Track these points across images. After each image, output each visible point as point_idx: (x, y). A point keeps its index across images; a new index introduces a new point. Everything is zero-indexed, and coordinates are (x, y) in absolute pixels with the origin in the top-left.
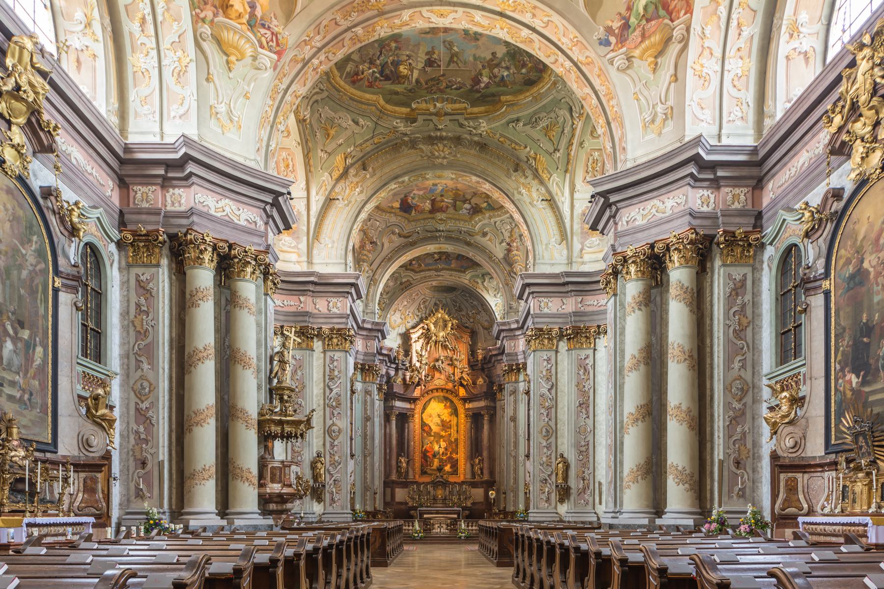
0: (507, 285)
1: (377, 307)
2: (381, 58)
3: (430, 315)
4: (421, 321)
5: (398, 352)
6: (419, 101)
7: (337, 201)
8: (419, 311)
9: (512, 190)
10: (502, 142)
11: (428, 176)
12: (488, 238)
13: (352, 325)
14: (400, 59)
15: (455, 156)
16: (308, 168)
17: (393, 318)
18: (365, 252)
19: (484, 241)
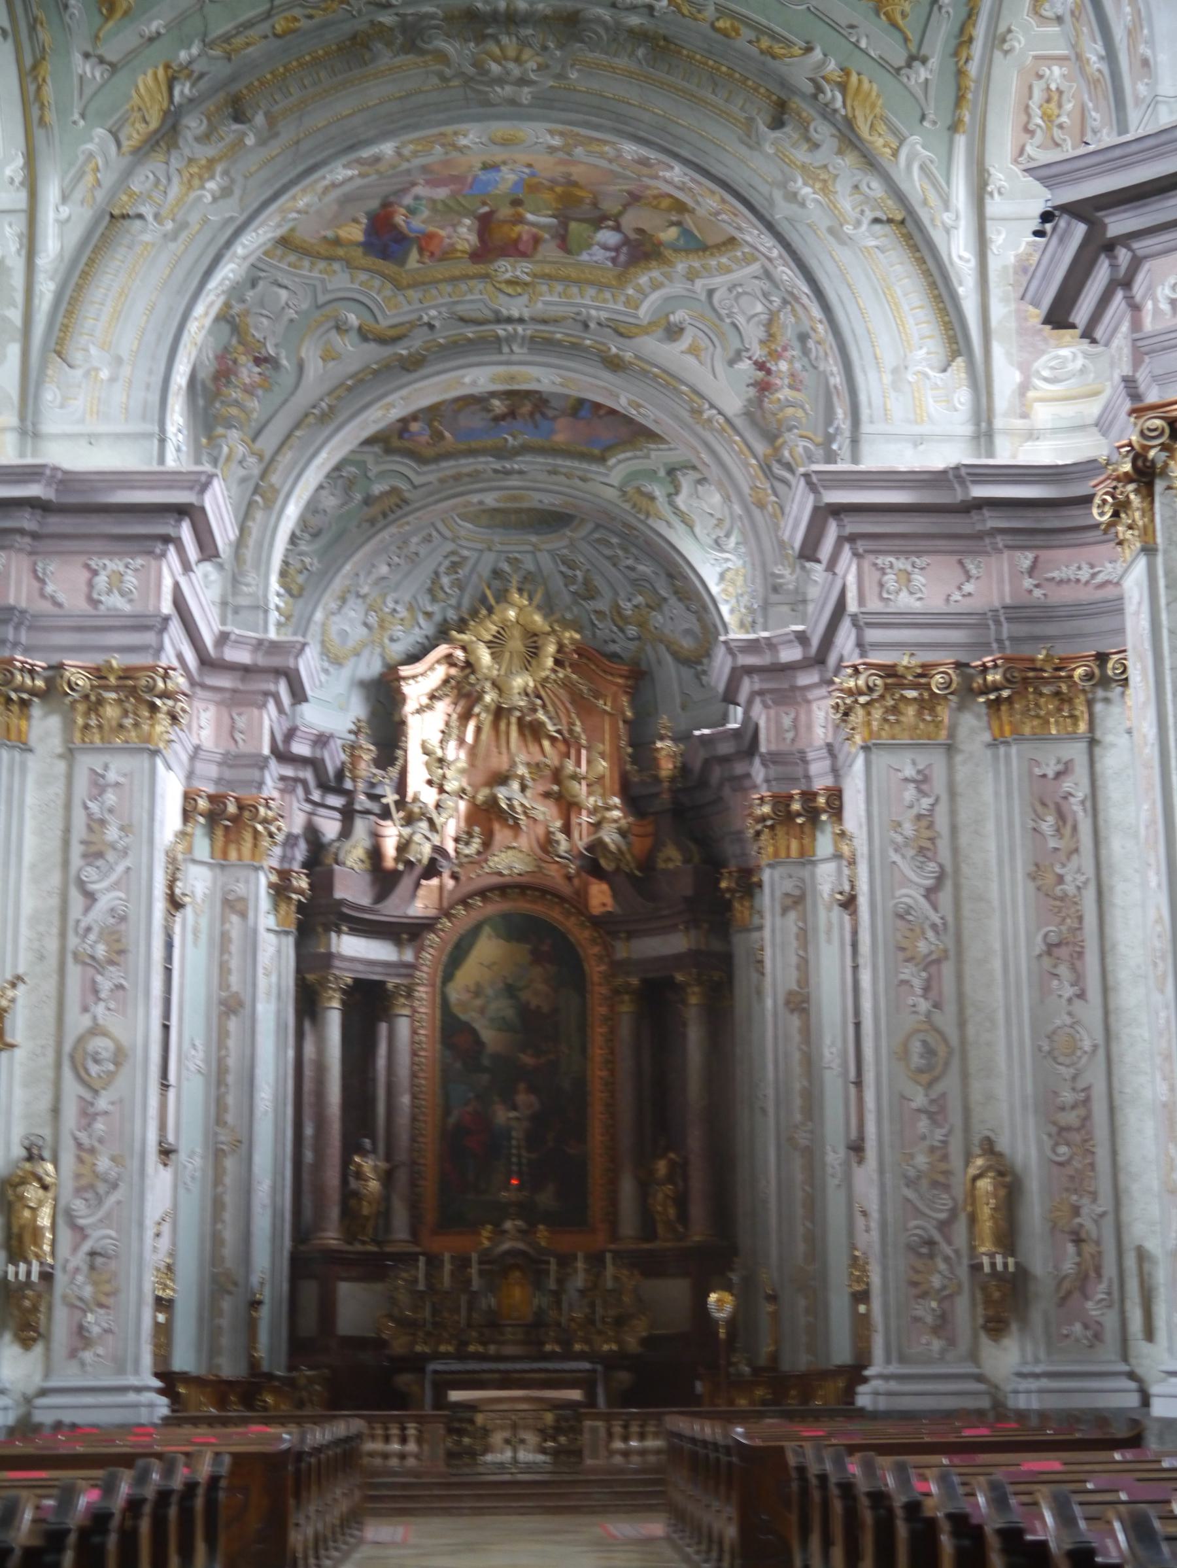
0: (761, 506)
1: (274, 585)
3: (474, 613)
4: (442, 634)
5: (352, 749)
7: (138, 223)
8: (434, 599)
9: (764, 189)
10: (724, 33)
11: (463, 141)
12: (685, 342)
13: (180, 657)
15: (561, 76)
16: (35, 113)
17: (338, 624)
18: (235, 394)
19: (671, 354)
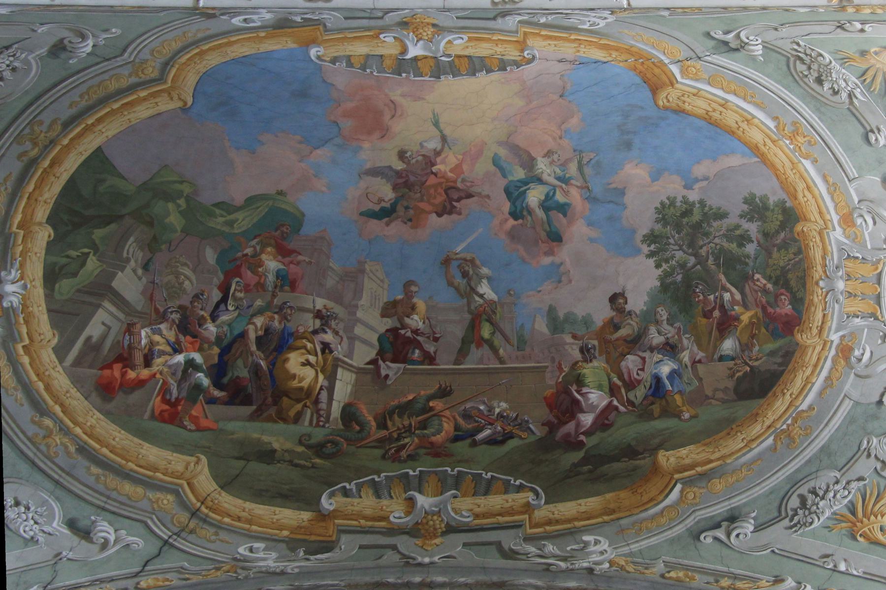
2: (224, 318)
6: (351, 486)
14: (291, 326)
